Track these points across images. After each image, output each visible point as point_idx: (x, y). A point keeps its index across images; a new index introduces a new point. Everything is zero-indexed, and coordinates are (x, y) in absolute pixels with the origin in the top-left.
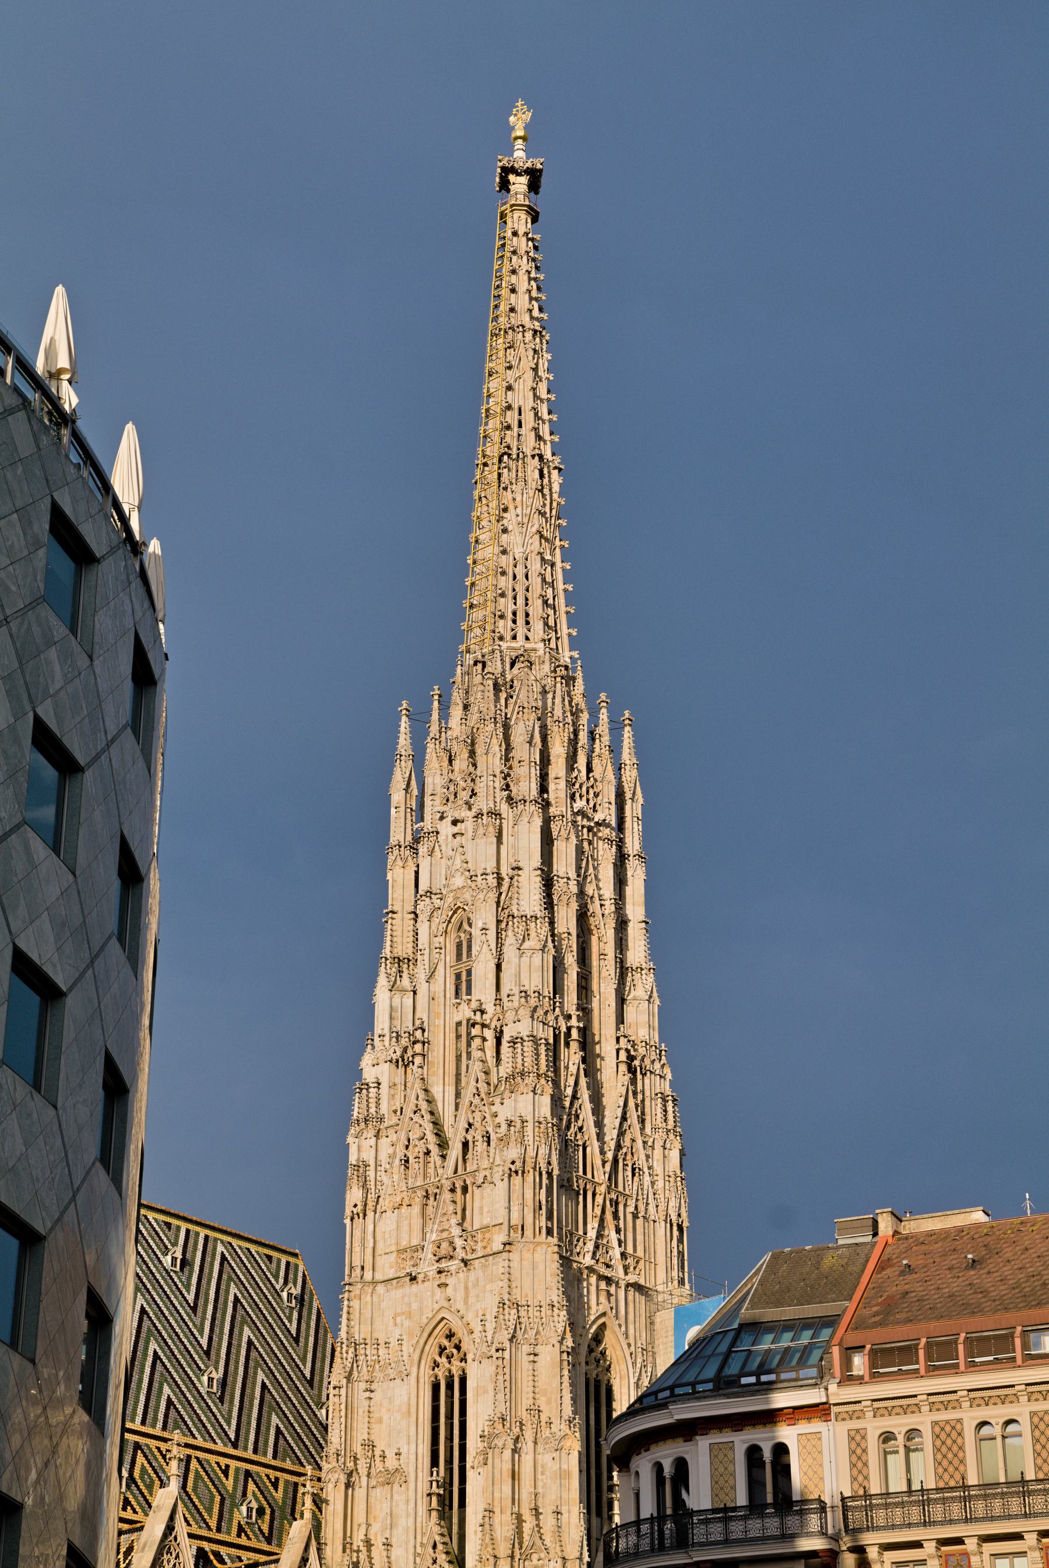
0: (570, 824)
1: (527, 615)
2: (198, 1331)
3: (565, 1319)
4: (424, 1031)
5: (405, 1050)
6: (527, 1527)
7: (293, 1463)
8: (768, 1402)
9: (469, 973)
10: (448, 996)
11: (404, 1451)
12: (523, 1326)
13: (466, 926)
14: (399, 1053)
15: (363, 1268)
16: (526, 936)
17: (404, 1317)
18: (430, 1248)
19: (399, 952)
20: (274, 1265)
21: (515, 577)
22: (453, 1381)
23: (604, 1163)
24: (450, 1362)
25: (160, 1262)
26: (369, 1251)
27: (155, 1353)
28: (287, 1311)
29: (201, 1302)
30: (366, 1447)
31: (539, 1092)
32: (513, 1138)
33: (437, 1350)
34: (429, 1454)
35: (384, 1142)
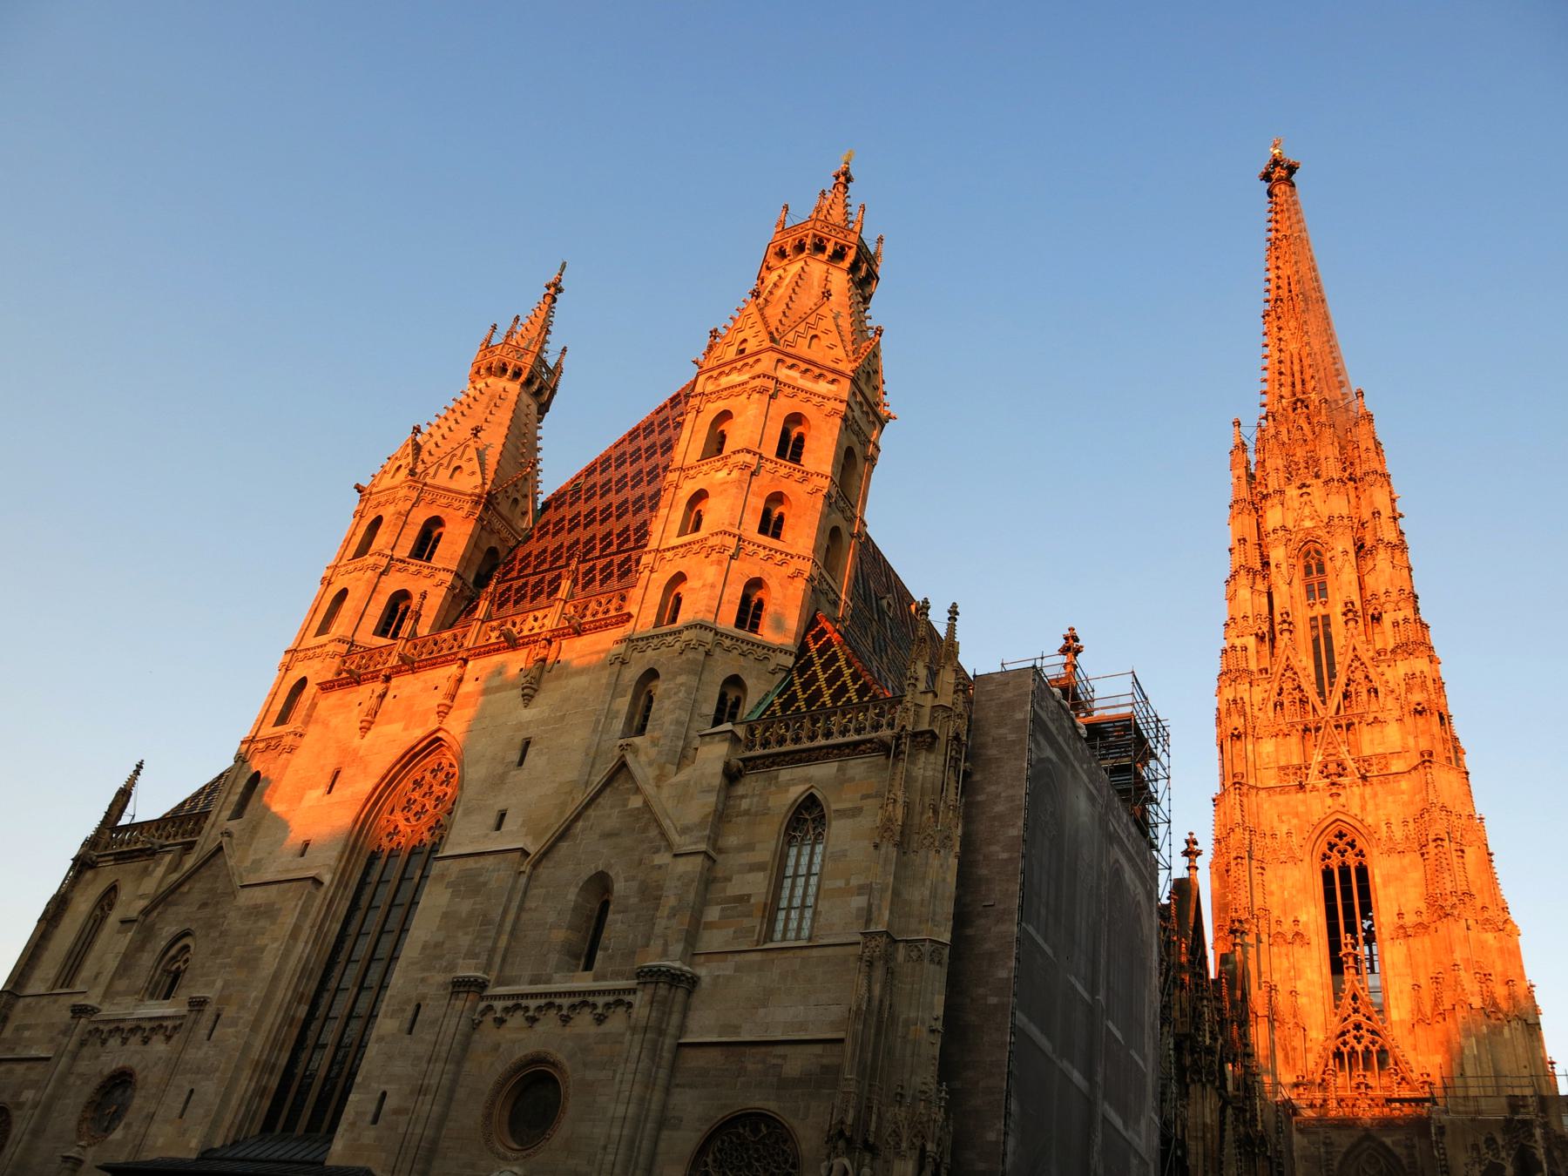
4: (1288, 616)
11: (1303, 918)
13: (1313, 553)
24: (1343, 856)
33: (1325, 847)
35: (1255, 688)
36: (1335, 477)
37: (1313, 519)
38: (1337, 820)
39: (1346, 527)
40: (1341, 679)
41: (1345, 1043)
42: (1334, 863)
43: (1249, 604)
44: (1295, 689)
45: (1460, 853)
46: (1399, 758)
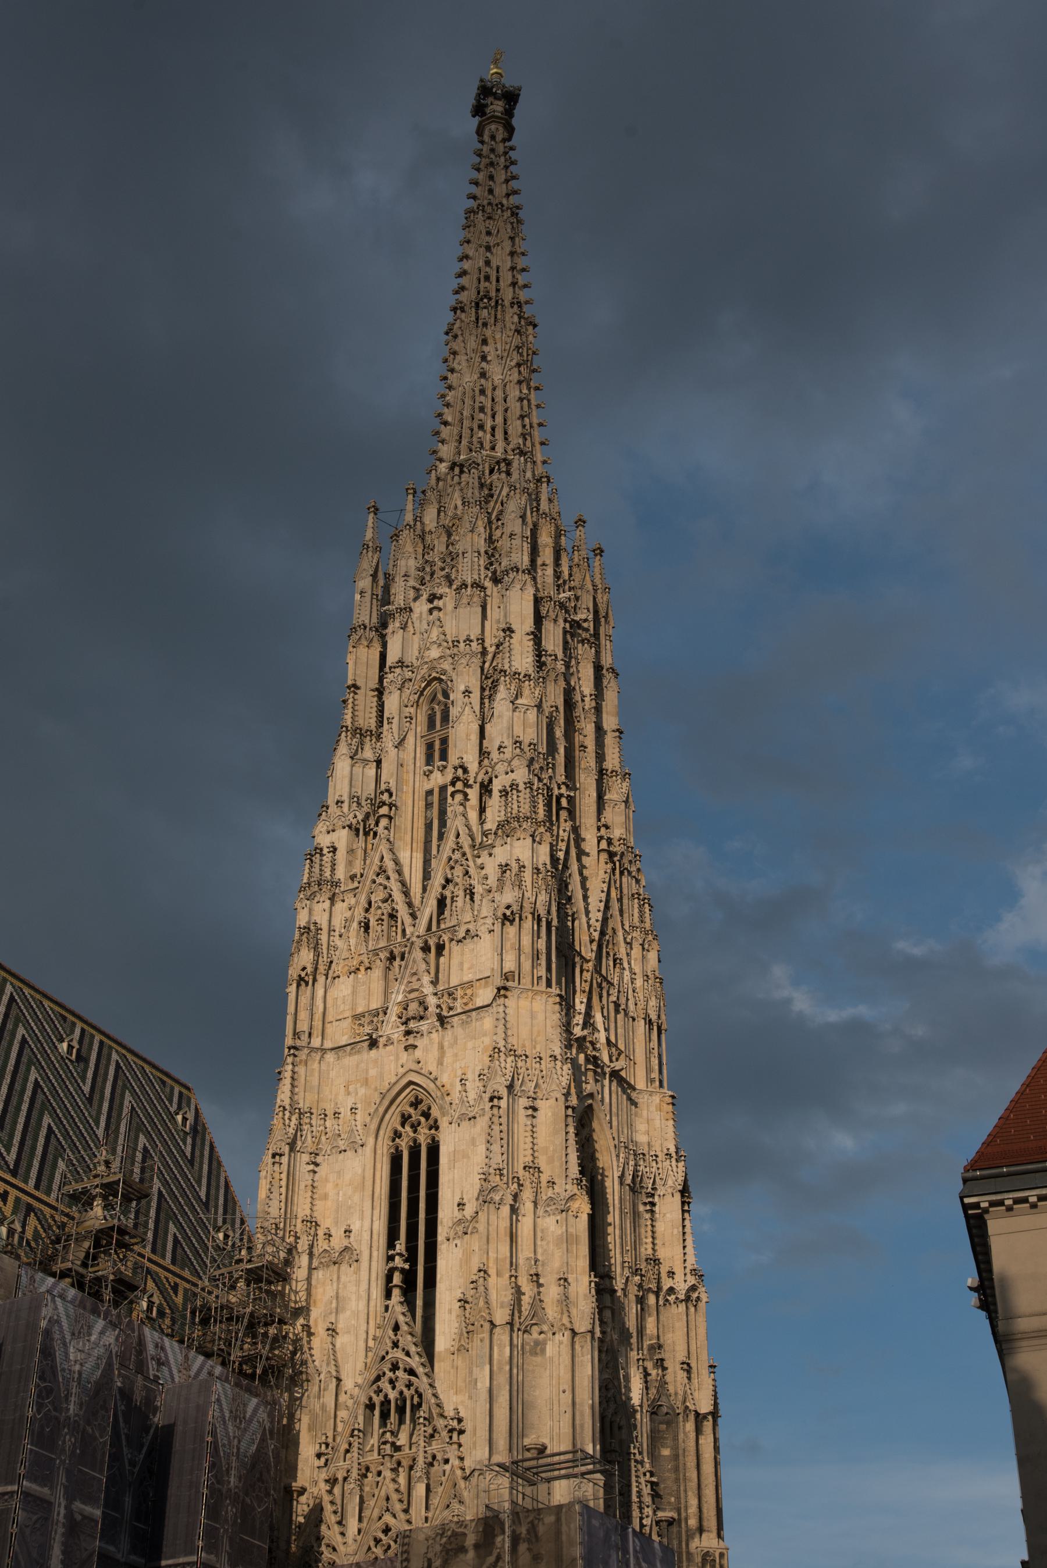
0: (558, 607)
1: (506, 433)
2: (94, 1121)
3: (570, 1072)
4: (391, 795)
5: (367, 816)
6: (526, 1300)
7: (191, 1274)
8: (421, 1496)
9: (444, 741)
10: (418, 764)
11: (355, 1227)
12: (521, 1077)
14: (360, 817)
15: (310, 1034)
16: (518, 695)
17: (359, 1085)
18: (394, 1011)
19: (361, 722)
20: (168, 1090)
21: (493, 400)
22: (420, 1151)
23: (592, 941)
24: (415, 1131)
25: (56, 1047)
26: (318, 1016)
27: (49, 1127)
28: (181, 1134)
29: (96, 1097)
30: (309, 1224)
31: (537, 839)
32: (508, 883)
33: (399, 1119)
34: (386, 1232)
35: (339, 906)
36: (469, 582)
37: (440, 645)
38: (411, 1083)
39: (473, 655)
40: (438, 880)
41: (379, 1391)
42: (403, 1144)
43: (347, 781)
44: (385, 901)
45: (530, 1112)
46: (486, 985)
